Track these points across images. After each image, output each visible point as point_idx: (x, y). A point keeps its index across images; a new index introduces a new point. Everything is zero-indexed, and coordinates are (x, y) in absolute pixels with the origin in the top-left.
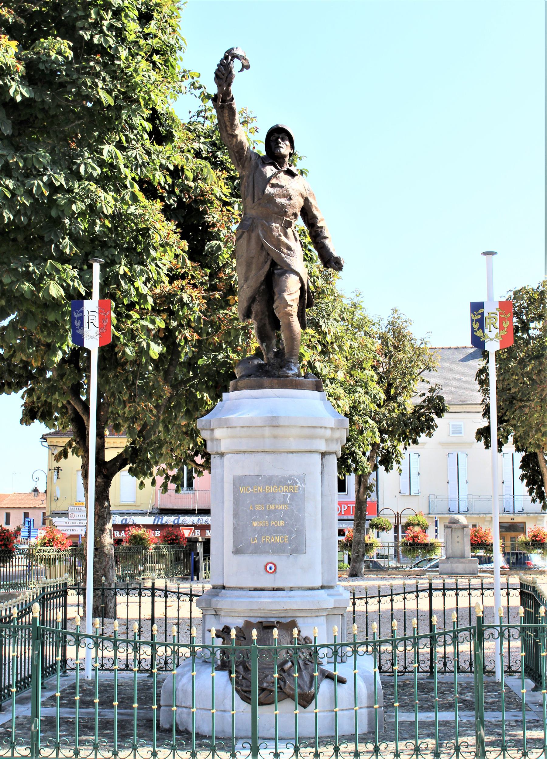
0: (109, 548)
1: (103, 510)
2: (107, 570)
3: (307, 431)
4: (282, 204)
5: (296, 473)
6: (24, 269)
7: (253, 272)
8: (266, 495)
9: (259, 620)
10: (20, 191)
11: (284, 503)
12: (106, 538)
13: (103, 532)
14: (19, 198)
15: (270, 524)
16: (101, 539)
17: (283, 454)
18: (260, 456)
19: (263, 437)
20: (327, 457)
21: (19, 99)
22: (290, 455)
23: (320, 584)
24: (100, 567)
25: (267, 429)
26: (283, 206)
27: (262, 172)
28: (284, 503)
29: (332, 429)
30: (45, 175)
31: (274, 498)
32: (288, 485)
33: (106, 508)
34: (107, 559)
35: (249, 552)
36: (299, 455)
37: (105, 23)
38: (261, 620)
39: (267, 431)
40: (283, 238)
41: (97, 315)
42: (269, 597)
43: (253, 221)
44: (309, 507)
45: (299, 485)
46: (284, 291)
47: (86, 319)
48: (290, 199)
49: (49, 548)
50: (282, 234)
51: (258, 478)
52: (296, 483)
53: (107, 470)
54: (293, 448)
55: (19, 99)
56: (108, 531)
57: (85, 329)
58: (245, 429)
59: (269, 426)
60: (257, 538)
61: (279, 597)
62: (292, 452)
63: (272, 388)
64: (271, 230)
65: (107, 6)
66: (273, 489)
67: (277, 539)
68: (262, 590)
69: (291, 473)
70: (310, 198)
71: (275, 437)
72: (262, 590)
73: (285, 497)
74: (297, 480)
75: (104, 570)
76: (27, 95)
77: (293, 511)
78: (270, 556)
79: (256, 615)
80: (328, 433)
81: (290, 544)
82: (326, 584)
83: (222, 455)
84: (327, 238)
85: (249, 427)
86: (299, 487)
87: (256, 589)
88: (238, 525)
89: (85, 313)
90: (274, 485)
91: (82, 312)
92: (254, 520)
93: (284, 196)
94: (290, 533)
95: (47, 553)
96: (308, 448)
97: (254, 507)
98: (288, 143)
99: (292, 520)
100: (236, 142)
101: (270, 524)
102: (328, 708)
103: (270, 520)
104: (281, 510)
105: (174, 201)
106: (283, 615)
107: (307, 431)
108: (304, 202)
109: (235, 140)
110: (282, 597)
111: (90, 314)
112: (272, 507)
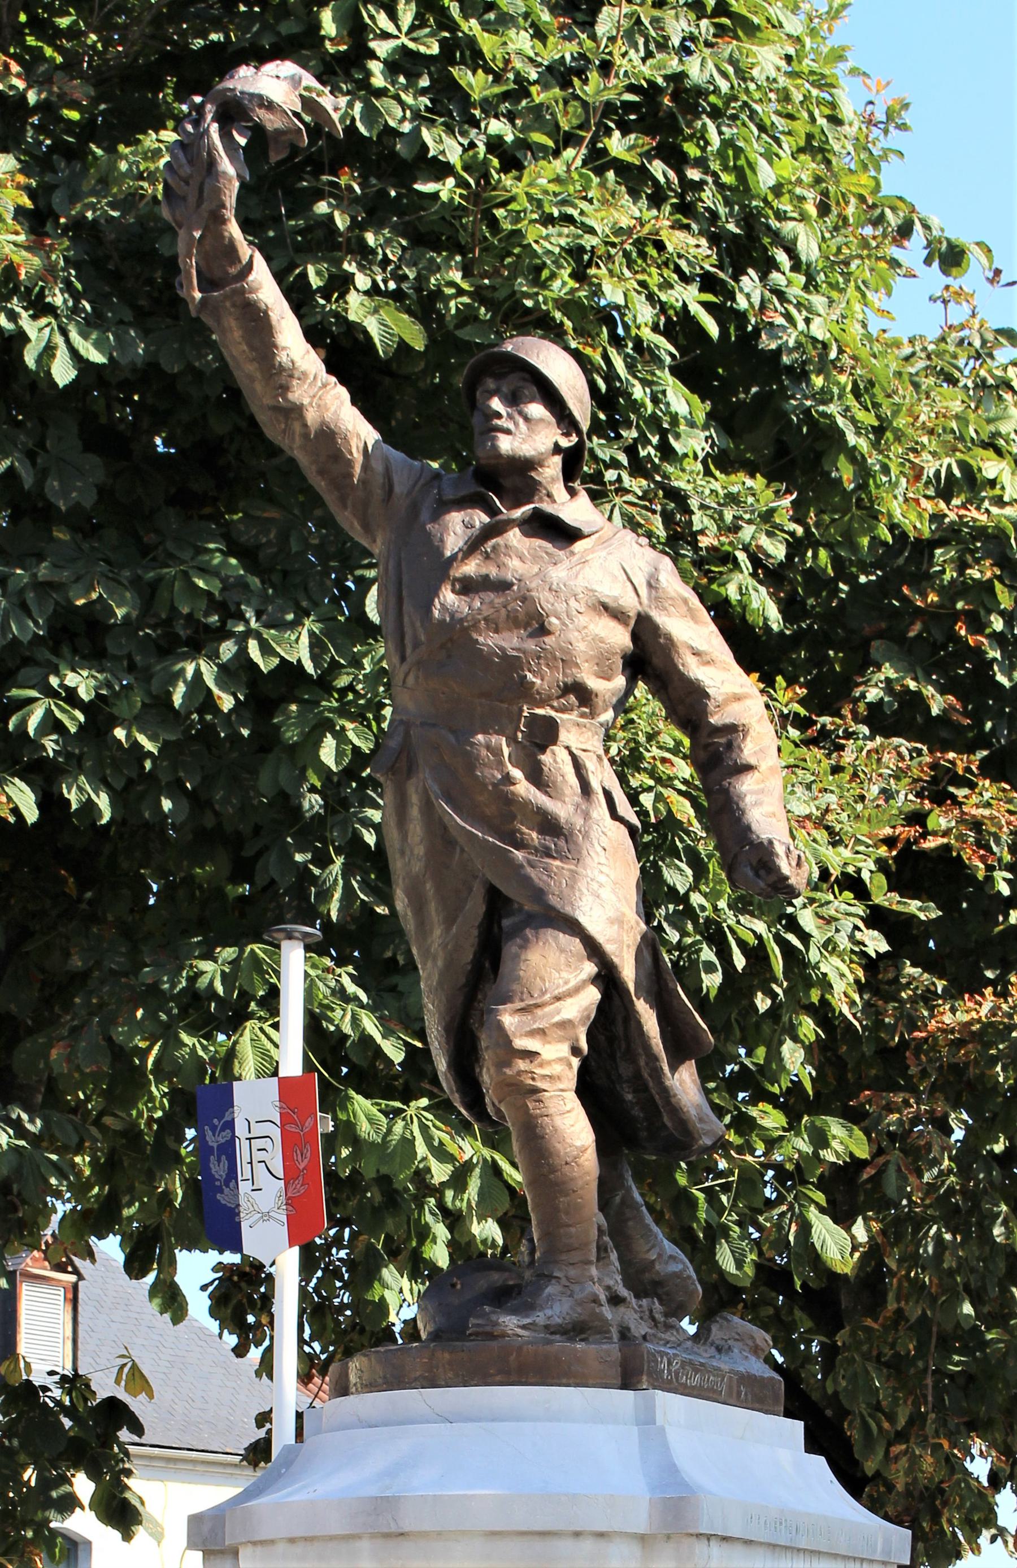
4: (505, 656)
7: (437, 932)
10: (131, 705)
14: (120, 733)
21: (63, 373)
27: (428, 535)
29: (642, 1539)
30: (228, 635)
37: (382, 48)
40: (523, 788)
41: (276, 1133)
43: (407, 734)
46: (506, 1000)
48: (543, 630)
50: (517, 773)
55: (63, 373)
57: (244, 1187)
59: (373, 1536)
63: (432, 1383)
64: (471, 762)
76: (97, 357)
84: (748, 768)
91: (231, 1125)
93: (514, 622)
98: (536, 410)
100: (306, 435)
108: (635, 637)
109: (297, 427)
111: (258, 1130)
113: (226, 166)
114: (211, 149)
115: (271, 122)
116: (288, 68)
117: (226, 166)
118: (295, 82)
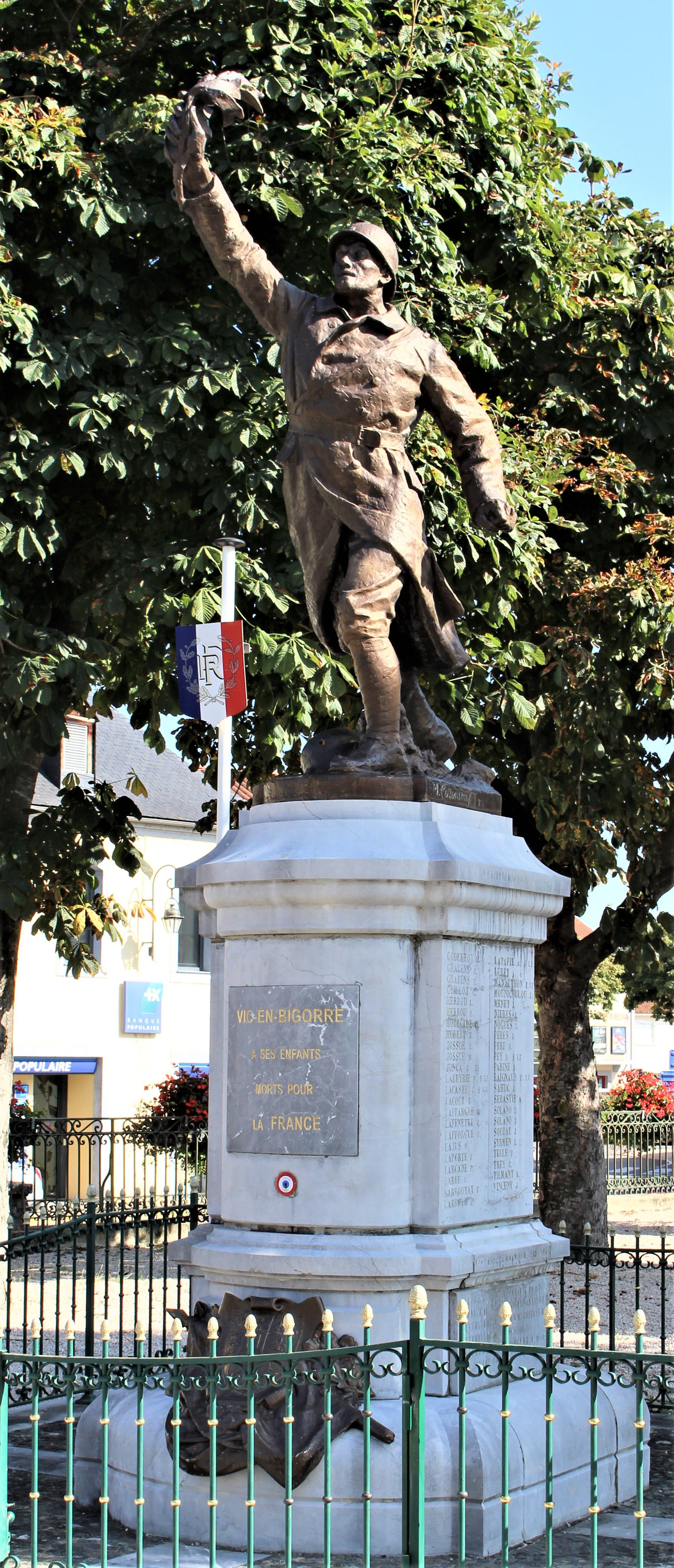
0: (586, 1118)
1: (571, 1040)
2: (582, 1163)
3: (355, 891)
4: (351, 399)
5: (339, 981)
6: (163, 567)
7: (313, 549)
8: (279, 1027)
9: (249, 1293)
10: (138, 413)
11: (314, 1044)
12: (580, 1098)
13: (574, 1087)
14: (131, 428)
15: (285, 1090)
16: (568, 1099)
17: (313, 941)
18: (270, 945)
19: (269, 903)
20: (426, 945)
21: (101, 229)
22: (328, 942)
23: (404, 1221)
24: (568, 1158)
25: (273, 886)
26: (355, 403)
27: (309, 331)
28: (314, 1044)
29: (425, 883)
30: (193, 374)
31: (294, 1035)
32: (323, 1007)
33: (577, 1036)
34: (583, 1141)
35: (250, 1149)
36: (348, 941)
37: (280, 50)
38: (258, 1294)
39: (274, 892)
40: (361, 471)
41: (220, 653)
42: (277, 1246)
43: (297, 441)
44: (370, 1055)
45: (345, 1006)
46: (351, 587)
47: (201, 663)
48: (372, 385)
49: (630, 1113)
50: (357, 463)
51: (266, 992)
52: (339, 1002)
53: (576, 957)
54: (331, 927)
55: (101, 229)
56: (585, 1083)
57: (202, 683)
58: (237, 888)
59: (278, 881)
60: (263, 1119)
61: (293, 1247)
62: (332, 936)
63: (309, 797)
64: (332, 456)
65: (283, 15)
66: (291, 1015)
67: (299, 1124)
68: (272, 1229)
69: (328, 981)
70: (436, 378)
71: (293, 904)
72: (272, 1229)
73: (315, 1032)
74: (342, 997)
75: (577, 1163)
76: (120, 220)
77: (331, 1063)
78: (285, 1158)
79: (245, 1282)
80: (414, 893)
81: (324, 1134)
82: (419, 1223)
83: (220, 940)
84: (484, 460)
85: (243, 883)
86: (346, 1011)
87: (262, 1229)
88: (234, 1090)
89: (200, 651)
90: (293, 1007)
91: (194, 649)
92: (259, 1081)
93: (356, 380)
94: (325, 1110)
95: (623, 1123)
96: (364, 927)
97: (258, 1052)
98: (369, 263)
99: (328, 1082)
100: (242, 276)
101: (285, 1090)
102: (348, 1493)
103: (285, 1082)
104: (307, 1061)
105: (639, 392)
106: (300, 1286)
107: (355, 891)
108: (422, 387)
109: (237, 271)
110: (302, 1247)
111: (209, 651)
112: (290, 1054)
113: (200, 129)
114: (191, 120)
115: (224, 105)
116: (234, 75)
117: (200, 129)
118: (238, 83)
